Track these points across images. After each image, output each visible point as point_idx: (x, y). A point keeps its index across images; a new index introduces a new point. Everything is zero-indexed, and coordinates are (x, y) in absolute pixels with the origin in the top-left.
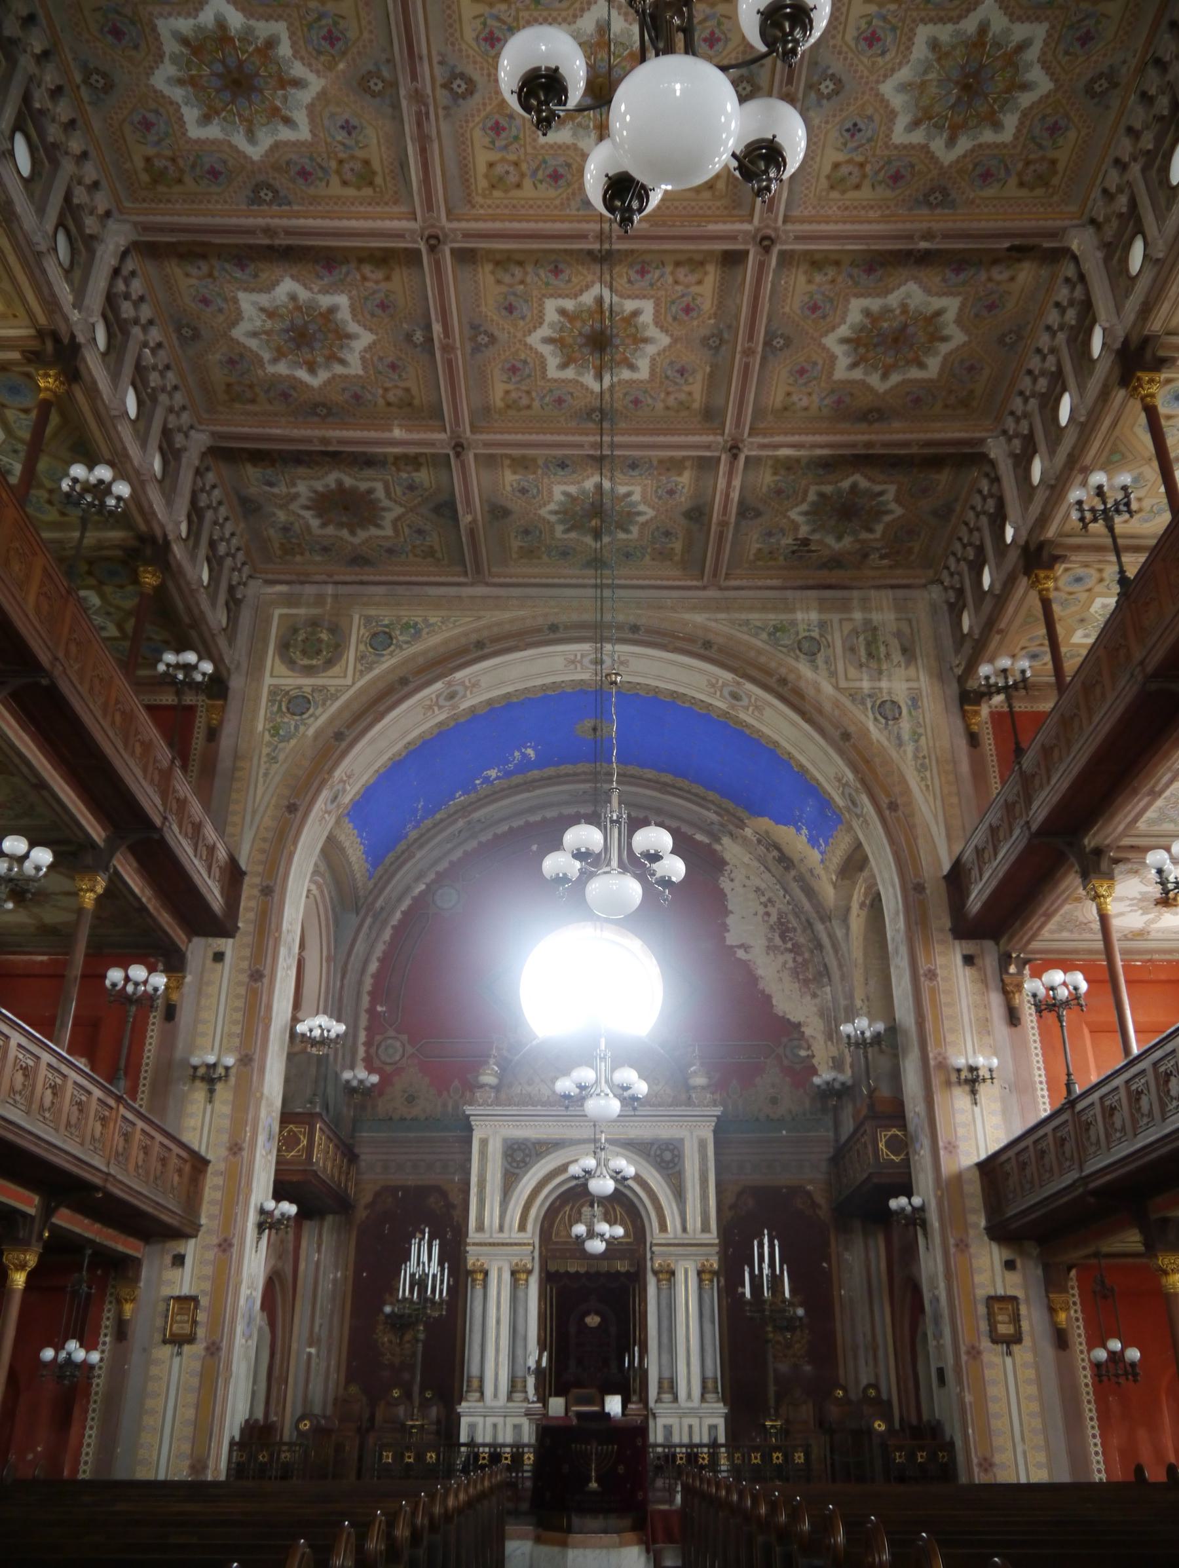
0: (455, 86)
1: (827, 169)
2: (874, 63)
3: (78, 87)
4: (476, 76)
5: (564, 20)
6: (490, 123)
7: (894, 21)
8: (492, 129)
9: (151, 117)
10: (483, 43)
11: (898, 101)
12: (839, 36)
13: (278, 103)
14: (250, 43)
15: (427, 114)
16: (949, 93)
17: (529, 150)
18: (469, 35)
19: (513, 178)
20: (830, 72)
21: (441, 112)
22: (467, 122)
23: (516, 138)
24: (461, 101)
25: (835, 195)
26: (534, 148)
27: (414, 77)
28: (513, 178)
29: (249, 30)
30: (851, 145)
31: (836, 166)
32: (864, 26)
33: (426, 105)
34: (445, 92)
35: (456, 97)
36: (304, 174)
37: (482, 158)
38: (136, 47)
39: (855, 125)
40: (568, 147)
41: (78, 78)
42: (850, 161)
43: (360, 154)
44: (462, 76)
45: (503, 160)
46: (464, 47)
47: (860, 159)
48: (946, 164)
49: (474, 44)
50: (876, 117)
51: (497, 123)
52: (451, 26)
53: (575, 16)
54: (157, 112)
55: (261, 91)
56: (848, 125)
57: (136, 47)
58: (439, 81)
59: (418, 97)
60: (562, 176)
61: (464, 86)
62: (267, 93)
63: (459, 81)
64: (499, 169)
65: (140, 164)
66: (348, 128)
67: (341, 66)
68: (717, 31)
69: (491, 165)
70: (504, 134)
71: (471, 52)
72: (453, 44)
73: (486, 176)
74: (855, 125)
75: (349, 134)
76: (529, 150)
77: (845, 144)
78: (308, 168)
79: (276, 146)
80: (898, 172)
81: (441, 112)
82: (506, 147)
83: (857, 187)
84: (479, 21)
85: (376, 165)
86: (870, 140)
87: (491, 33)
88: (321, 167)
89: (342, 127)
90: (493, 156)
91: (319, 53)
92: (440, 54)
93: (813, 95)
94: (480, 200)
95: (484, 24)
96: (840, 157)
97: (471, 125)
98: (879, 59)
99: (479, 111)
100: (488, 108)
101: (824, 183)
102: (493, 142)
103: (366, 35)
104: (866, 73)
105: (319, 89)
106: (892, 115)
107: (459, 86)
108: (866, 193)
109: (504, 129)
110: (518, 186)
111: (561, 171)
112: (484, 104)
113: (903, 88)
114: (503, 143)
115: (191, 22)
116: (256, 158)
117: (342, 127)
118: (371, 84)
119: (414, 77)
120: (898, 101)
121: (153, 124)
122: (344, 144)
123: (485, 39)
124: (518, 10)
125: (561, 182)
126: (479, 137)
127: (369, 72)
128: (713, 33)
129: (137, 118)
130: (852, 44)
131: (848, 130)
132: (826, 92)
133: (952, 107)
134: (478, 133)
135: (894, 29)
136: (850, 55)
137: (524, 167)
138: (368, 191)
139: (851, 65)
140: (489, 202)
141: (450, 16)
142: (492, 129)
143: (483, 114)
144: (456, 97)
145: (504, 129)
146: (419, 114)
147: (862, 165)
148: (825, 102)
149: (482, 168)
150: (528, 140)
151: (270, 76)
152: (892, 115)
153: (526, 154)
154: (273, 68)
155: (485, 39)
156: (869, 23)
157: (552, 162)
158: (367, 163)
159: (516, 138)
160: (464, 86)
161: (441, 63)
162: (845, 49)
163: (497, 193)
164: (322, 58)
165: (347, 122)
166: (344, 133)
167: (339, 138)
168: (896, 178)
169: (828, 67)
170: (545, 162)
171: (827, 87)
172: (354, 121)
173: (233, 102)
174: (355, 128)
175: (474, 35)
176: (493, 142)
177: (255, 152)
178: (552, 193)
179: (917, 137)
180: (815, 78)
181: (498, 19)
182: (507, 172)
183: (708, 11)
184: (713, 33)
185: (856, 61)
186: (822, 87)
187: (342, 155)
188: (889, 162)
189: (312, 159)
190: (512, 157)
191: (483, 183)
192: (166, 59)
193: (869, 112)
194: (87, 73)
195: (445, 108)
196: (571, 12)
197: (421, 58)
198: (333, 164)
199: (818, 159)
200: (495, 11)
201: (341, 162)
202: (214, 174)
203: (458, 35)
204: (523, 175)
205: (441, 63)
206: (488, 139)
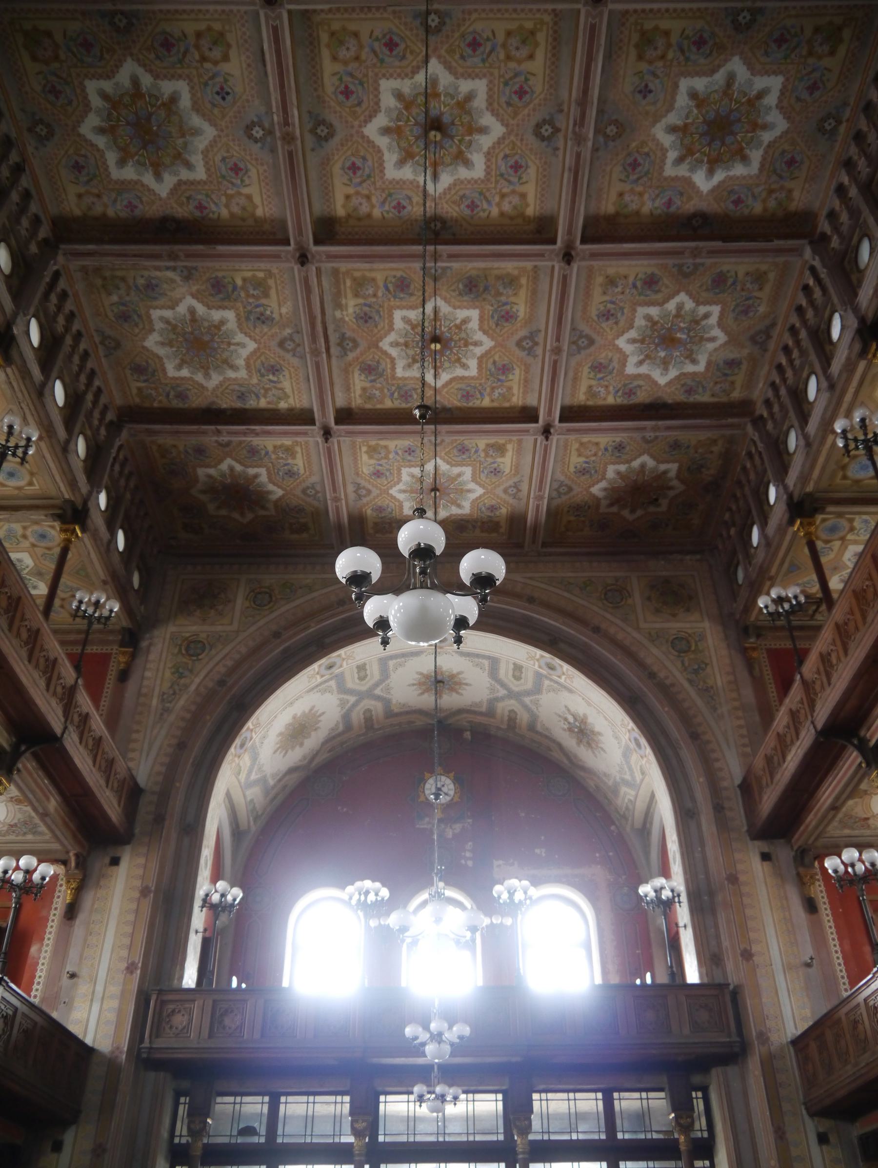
0: (550, 130)
1: (233, 53)
2: (228, 151)
3: (848, 120)
4: (531, 138)
5: (462, 182)
6: (527, 98)
7: (225, 183)
8: (526, 93)
9: (805, 95)
10: (523, 164)
11: (196, 121)
12: (261, 171)
13: (695, 111)
14: (696, 160)
15: (575, 124)
16: (159, 126)
17: (496, 72)
18: (532, 172)
19: (514, 42)
20: (259, 145)
21: (566, 109)
22: (545, 99)
23: (506, 84)
24: (547, 118)
25: (217, 26)
26: (492, 74)
27: (578, 155)
28: (514, 42)
29: (692, 170)
30: (220, 79)
31: (226, 58)
32: (245, 178)
33: (574, 132)
34: (558, 125)
35: (550, 122)
36: (700, 43)
37: (538, 65)
38: (784, 152)
39: (224, 99)
40: (462, 75)
41: (842, 129)
42: (216, 63)
43: (644, 66)
44: (543, 139)
45: (519, 62)
46: (537, 162)
47: (208, 65)
48: (129, 60)
49: (530, 163)
50: (209, 106)
51: (520, 98)
52: (545, 176)
53: (455, 185)
54: (798, 99)
55: (705, 121)
56: (229, 98)
57: (784, 152)
58: (561, 135)
59: (579, 139)
60: (469, 45)
61: (543, 130)
62: (701, 119)
63: (546, 134)
64: (524, 52)
65: (842, 50)
66: (645, 91)
67: (634, 145)
68: (352, 175)
69: (531, 57)
70: (516, 87)
71: (533, 157)
72: (545, 163)
73: (537, 45)
74: (224, 99)
75: (646, 86)
76: (496, 72)
77: (226, 81)
78: (694, 49)
79: (713, 71)
80: (169, 50)
81: (566, 109)
82: (516, 75)
83: (199, 35)
84: (524, 180)
85: (633, 53)
86: (206, 84)
87: (516, 172)
88: (682, 51)
89: (650, 91)
90: (528, 66)
91: (647, 154)
92: (557, 156)
93: (267, 125)
94: (547, 18)
95: (520, 178)
96: (225, 67)
97: (542, 96)
98: (225, 155)
99: (534, 110)
100: (526, 111)
101: (231, 38)
102: (527, 80)
103: (608, 169)
104: (231, 144)
105: (658, 125)
106: (197, 107)
107: (546, 131)
108: (190, 28)
109: (516, 92)
110: (509, 34)
111: (469, 51)
112: (529, 115)
113: (196, 132)
114: (517, 80)
115: (731, 173)
116: (736, 59)
117: (650, 91)
118: (615, 130)
119: (578, 155)
120: (196, 121)
121: (808, 88)
122: (655, 75)
123: (521, 167)
124: (495, 188)
125: (469, 39)
126: (538, 85)
127: (613, 141)
128: (354, 173)
129: (817, 94)
130: (250, 166)
131: (228, 93)
132: (257, 128)
133: (150, 115)
134: (538, 89)
135: (224, 177)
136: (248, 158)
137: (502, 56)
138: (649, 25)
139: (245, 150)
140: (538, 16)
141: (544, 183)
142: (526, 93)
143: (531, 106)
144: (550, 122)
145: (516, 92)
146: (582, 125)
147: (204, 59)
148: (255, 120)
149: (540, 54)
150: (496, 82)
151: (692, 134)
152: (197, 107)
153: (499, 68)
154: (687, 141)
155: (521, 167)
156: (242, 181)
157: (477, 60)
158: (640, 57)
159: (506, 84)
160: (543, 130)
161: (557, 149)
162: (254, 162)
163: (529, 25)
164: (646, 150)
165: (645, 97)
166: (651, 86)
167: (657, 81)
168: (167, 45)
169: (262, 148)
170: (483, 61)
171: (258, 132)
172: (639, 97)
173: (731, 111)
174: (640, 92)
175: (529, 171)
176: (527, 80)
177: (737, 66)
178: (479, 26)
179: (167, 87)
180: (269, 139)
181: (509, 182)
182: (517, 49)
183: (359, 189)
184: (354, 173)
185: (243, 153)
186: (261, 132)
187: (660, 64)
188: (181, 61)
189: (687, 59)
190: (512, 65)
191: (541, 37)
192: (766, 143)
193: (216, 111)
194: (834, 132)
195: (561, 111)
196: (458, 188)
197: (570, 169)
198: (670, 55)
199: (244, 66)
200: (511, 187)
201: (663, 57)
202: (781, 41)
203: (541, 170)
204: (504, 46)
205: (557, 149)
206: (530, 83)
